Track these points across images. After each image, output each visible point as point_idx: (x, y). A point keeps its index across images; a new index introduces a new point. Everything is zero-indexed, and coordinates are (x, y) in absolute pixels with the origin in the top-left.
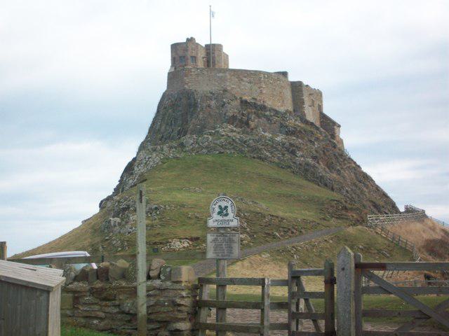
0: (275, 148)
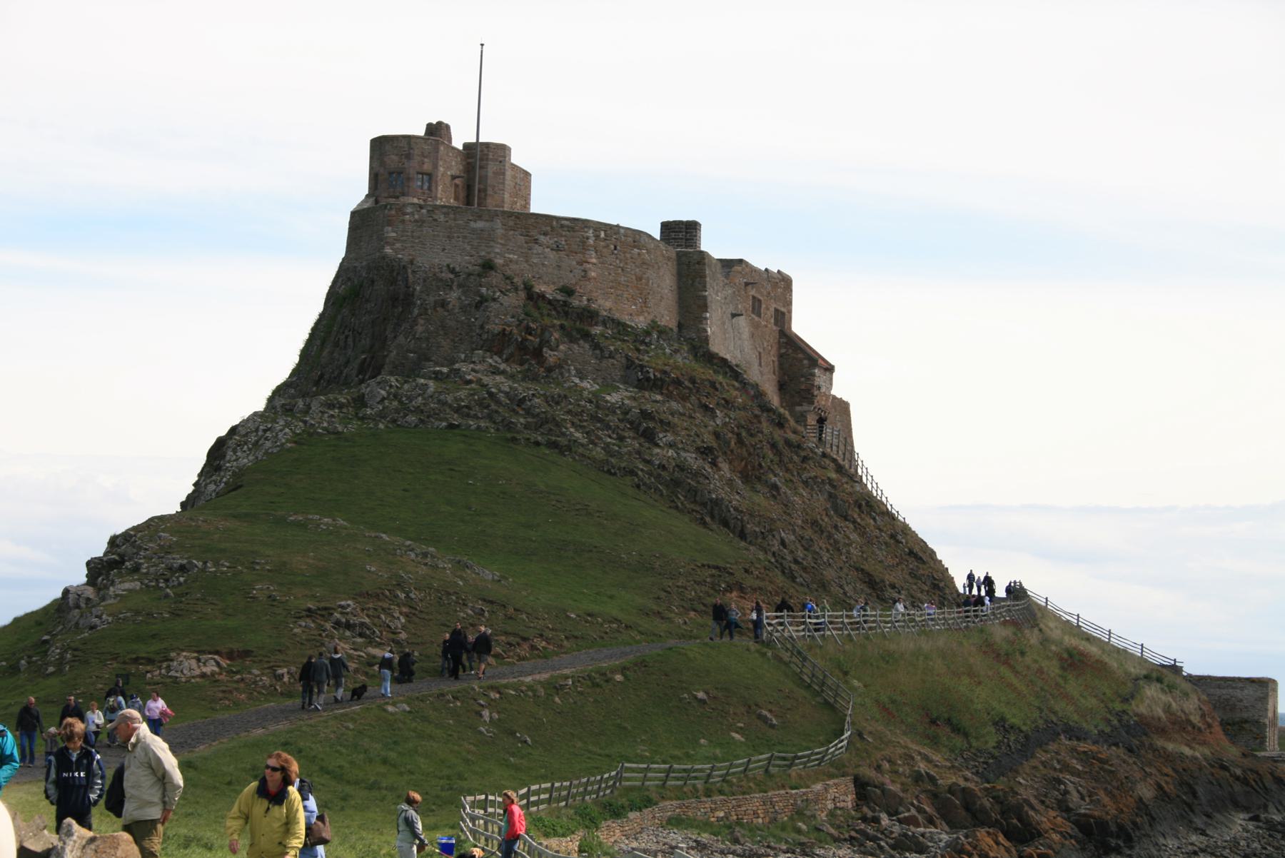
0: (600, 420)
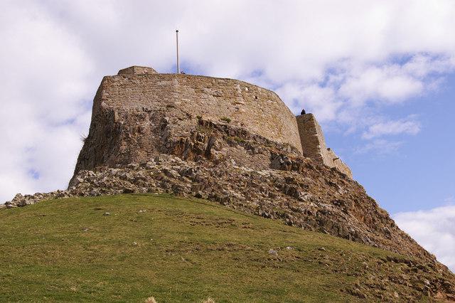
0: (255, 186)
